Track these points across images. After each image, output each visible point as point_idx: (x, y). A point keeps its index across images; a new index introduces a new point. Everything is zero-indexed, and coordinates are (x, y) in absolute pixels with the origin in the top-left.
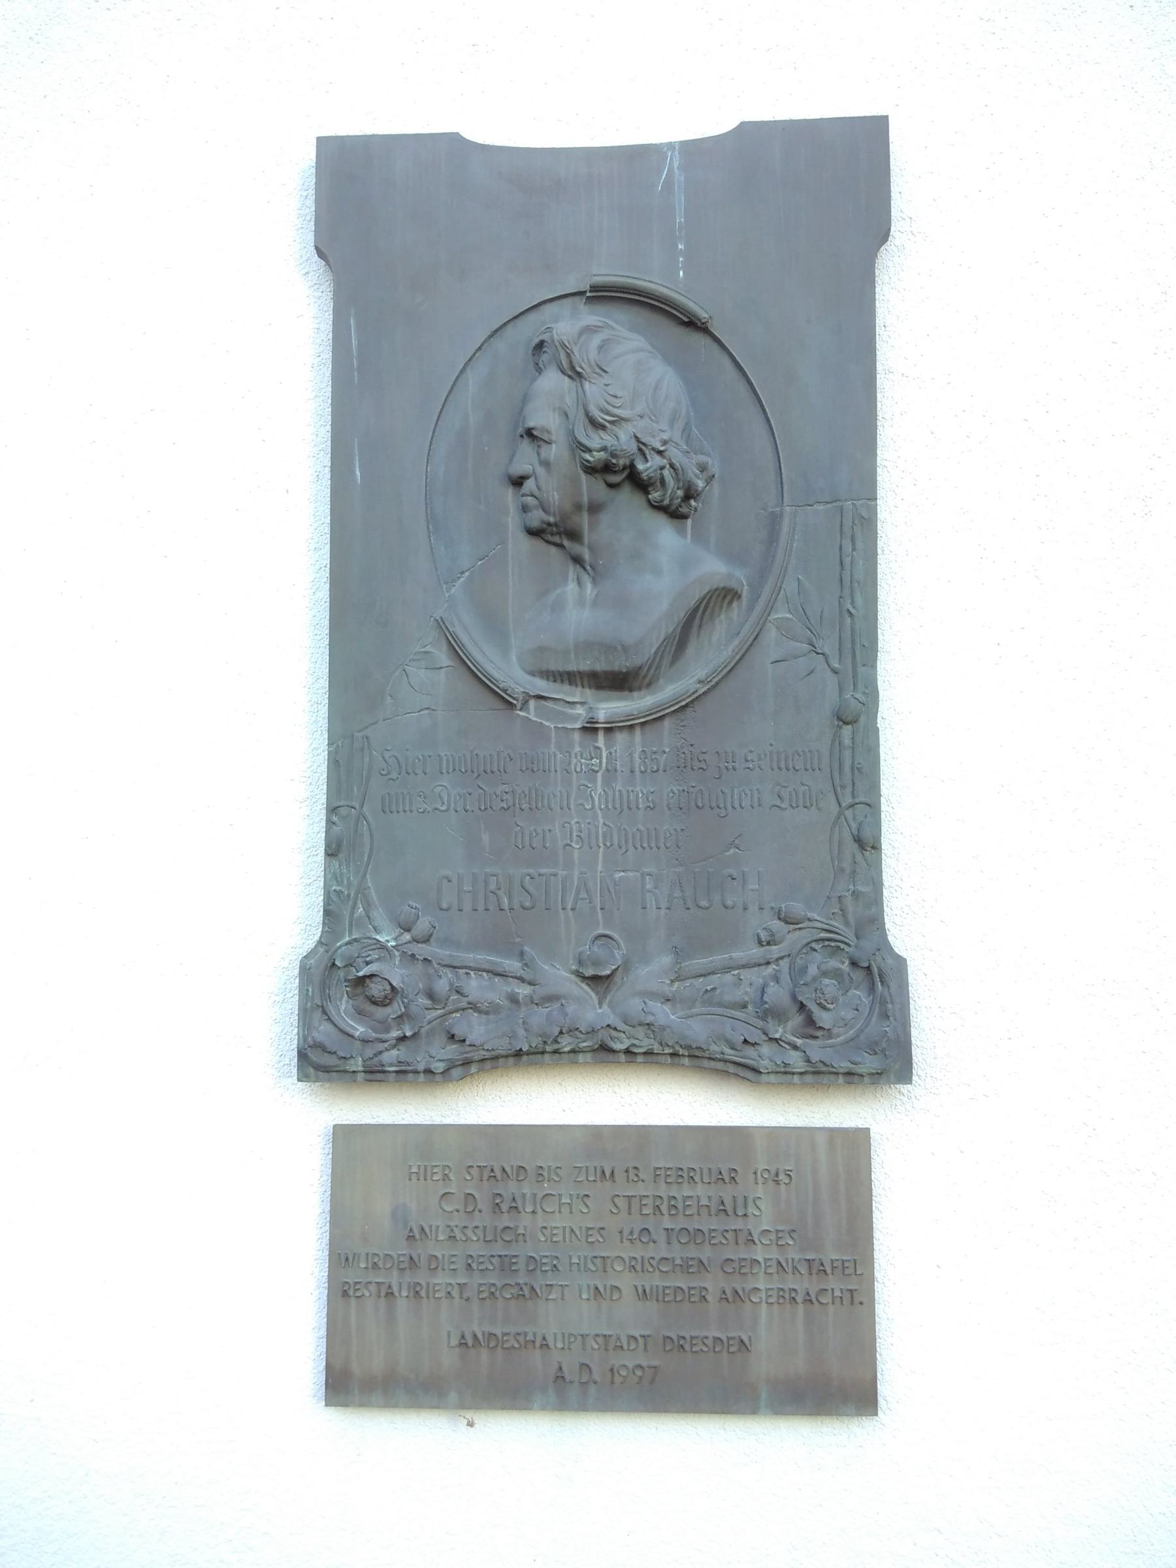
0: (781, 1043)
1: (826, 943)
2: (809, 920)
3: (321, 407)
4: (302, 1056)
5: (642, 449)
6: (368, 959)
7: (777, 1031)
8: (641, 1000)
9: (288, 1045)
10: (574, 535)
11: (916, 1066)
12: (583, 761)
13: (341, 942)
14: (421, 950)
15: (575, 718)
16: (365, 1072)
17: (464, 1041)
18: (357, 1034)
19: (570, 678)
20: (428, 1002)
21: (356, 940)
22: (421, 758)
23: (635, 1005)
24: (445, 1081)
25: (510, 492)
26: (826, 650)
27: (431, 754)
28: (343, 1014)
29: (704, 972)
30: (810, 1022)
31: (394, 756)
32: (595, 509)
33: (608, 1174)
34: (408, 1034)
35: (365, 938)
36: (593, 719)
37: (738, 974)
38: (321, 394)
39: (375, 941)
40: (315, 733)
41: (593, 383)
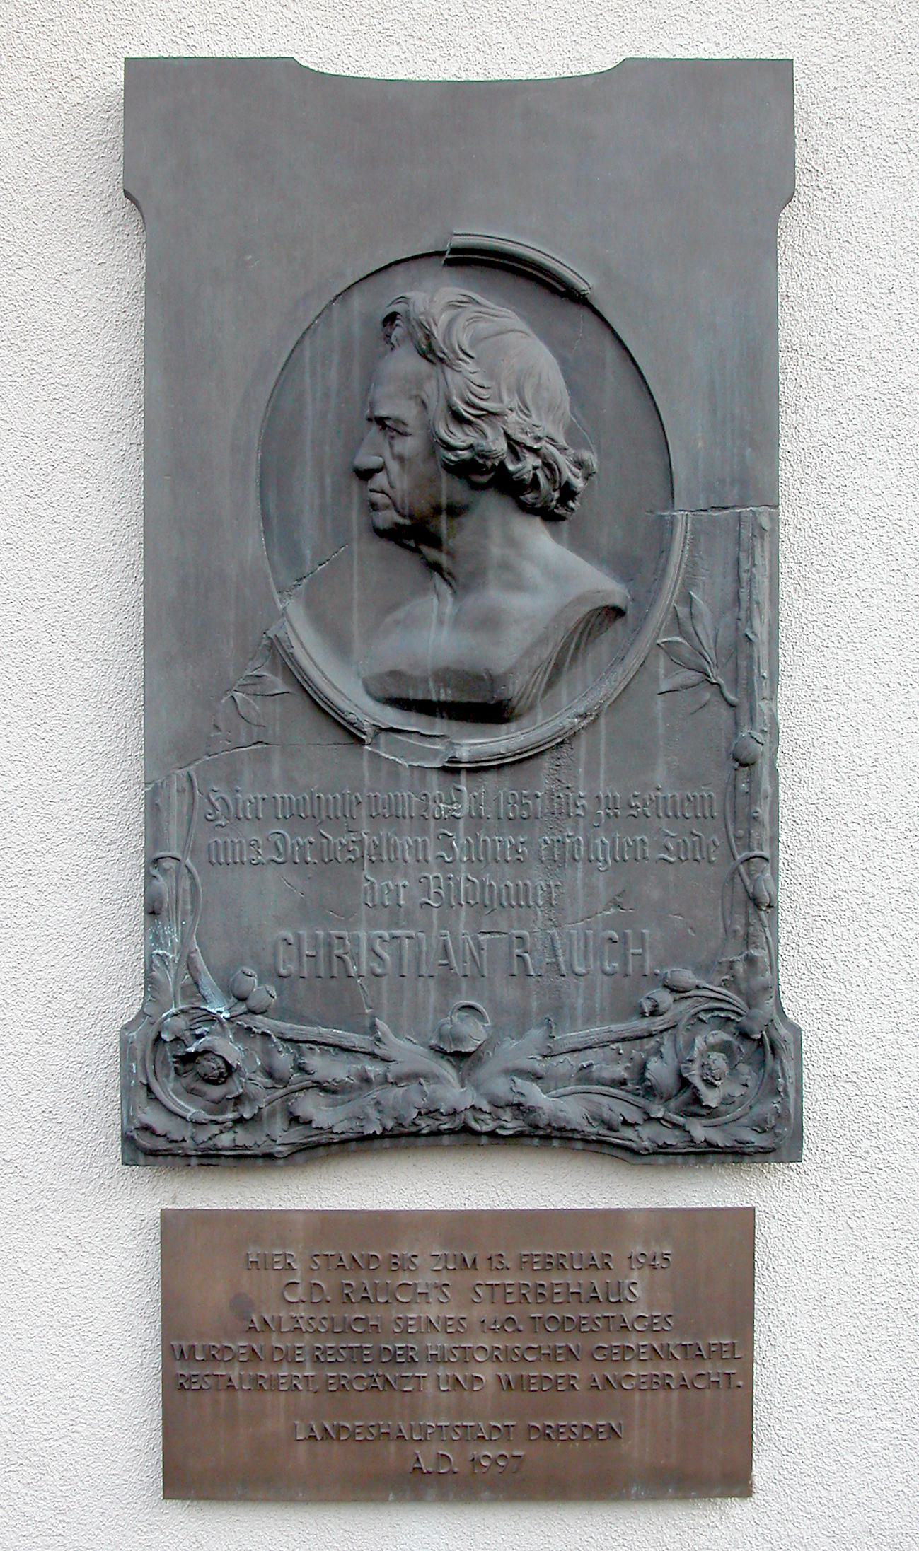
0: (662, 1122)
1: (716, 1013)
2: (698, 987)
3: (126, 373)
4: (127, 1139)
5: (515, 447)
6: (198, 1032)
7: (659, 1110)
8: (509, 1078)
9: (104, 1121)
10: (436, 543)
11: (807, 1140)
12: (442, 805)
13: (167, 1013)
14: (260, 1022)
15: (436, 753)
16: (197, 1156)
17: (310, 1122)
18: (189, 1115)
19: (426, 708)
20: (269, 1082)
21: (182, 1011)
22: (253, 800)
23: (501, 1087)
24: (287, 1165)
25: (355, 484)
26: (722, 682)
27: (266, 796)
28: (171, 1093)
29: (580, 1047)
30: (697, 1100)
31: (222, 798)
32: (454, 511)
33: (469, 1263)
34: (247, 1116)
35: (193, 1008)
36: (455, 757)
37: (618, 1049)
38: (127, 357)
39: (204, 1013)
40: (124, 763)
41: (457, 371)
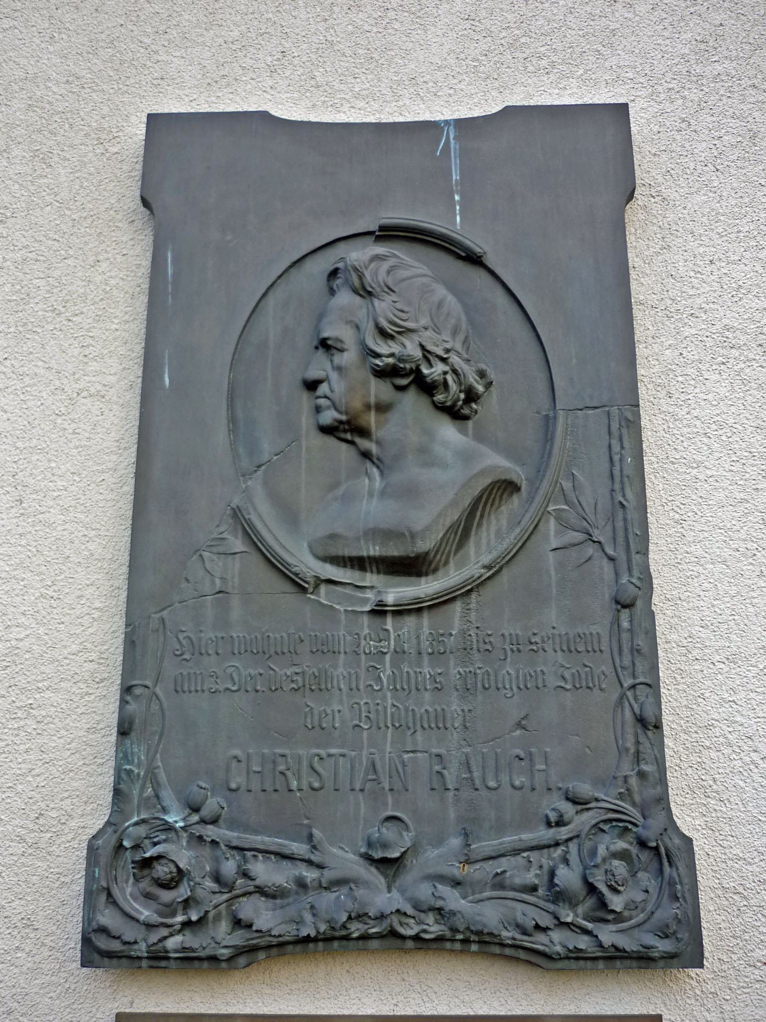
1: (614, 824)
2: (597, 800)
4: (86, 941)
6: (156, 840)
7: (568, 915)
8: (431, 884)
12: (372, 643)
14: (210, 832)
15: (365, 601)
16: (148, 958)
18: (142, 918)
19: (360, 563)
20: (214, 886)
21: (143, 821)
23: (424, 892)
24: (229, 969)
25: (305, 396)
26: (602, 539)
28: (129, 897)
29: (494, 854)
30: (603, 904)
32: (382, 408)
37: (528, 857)
39: (163, 822)
